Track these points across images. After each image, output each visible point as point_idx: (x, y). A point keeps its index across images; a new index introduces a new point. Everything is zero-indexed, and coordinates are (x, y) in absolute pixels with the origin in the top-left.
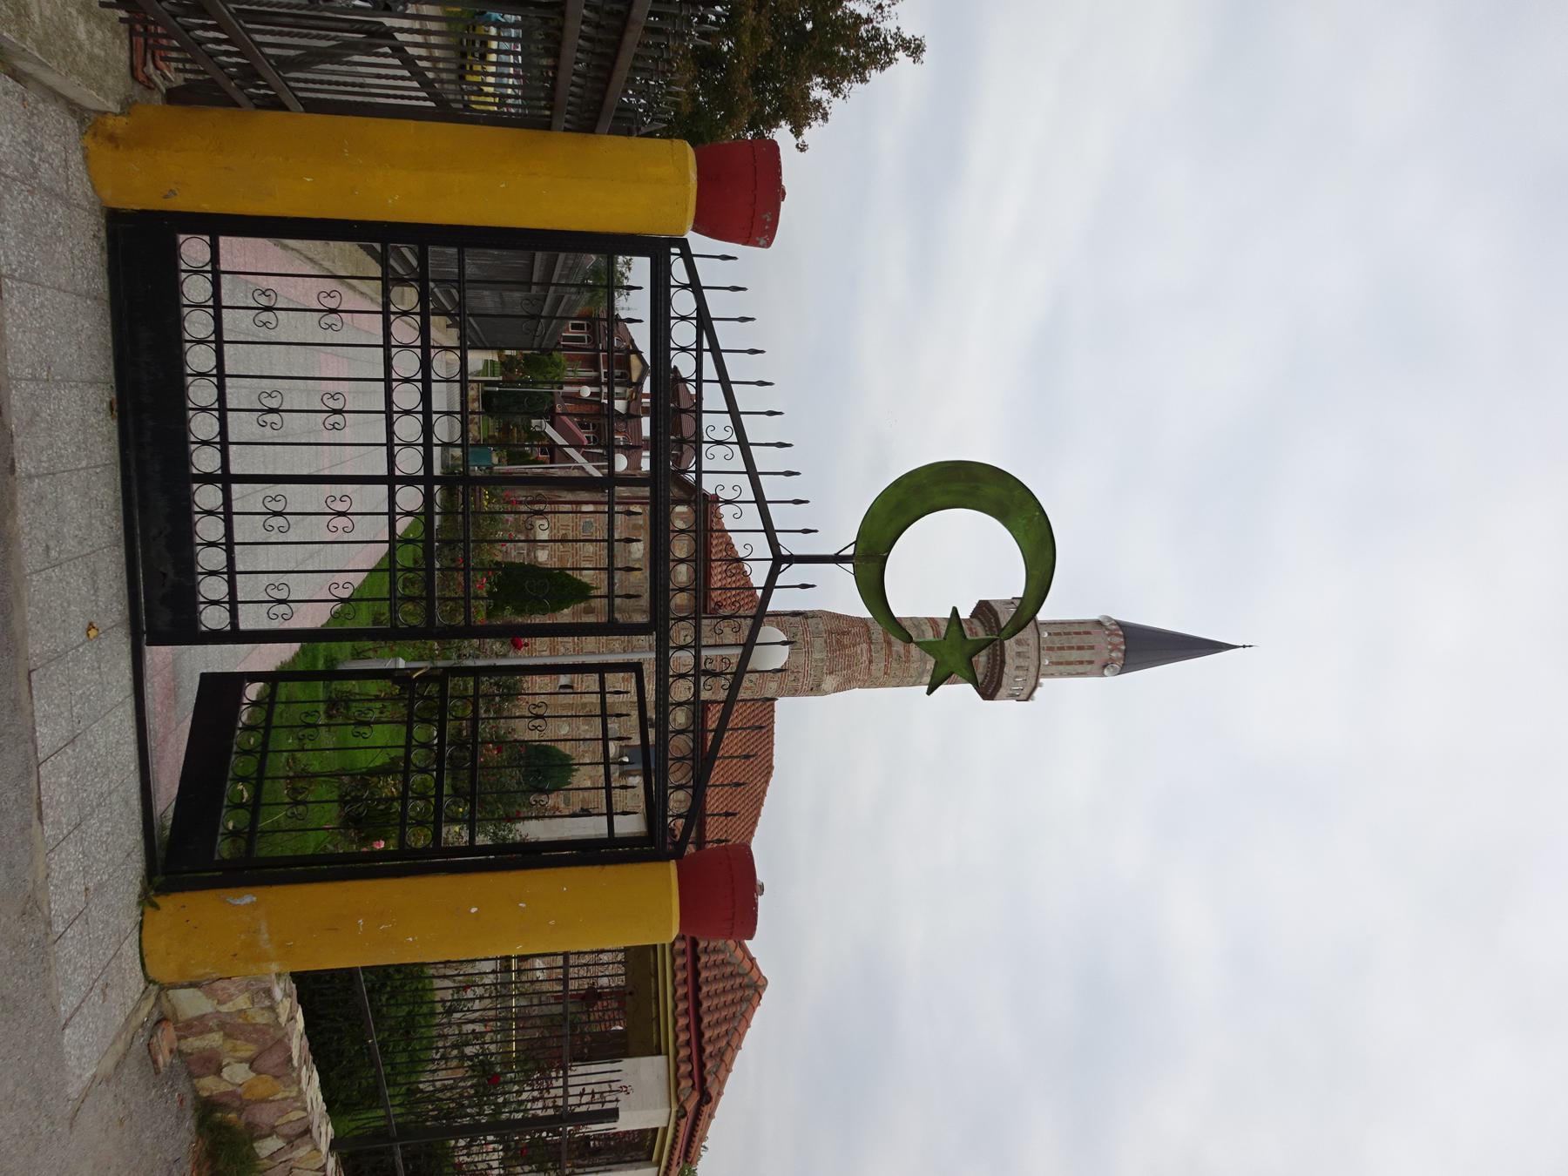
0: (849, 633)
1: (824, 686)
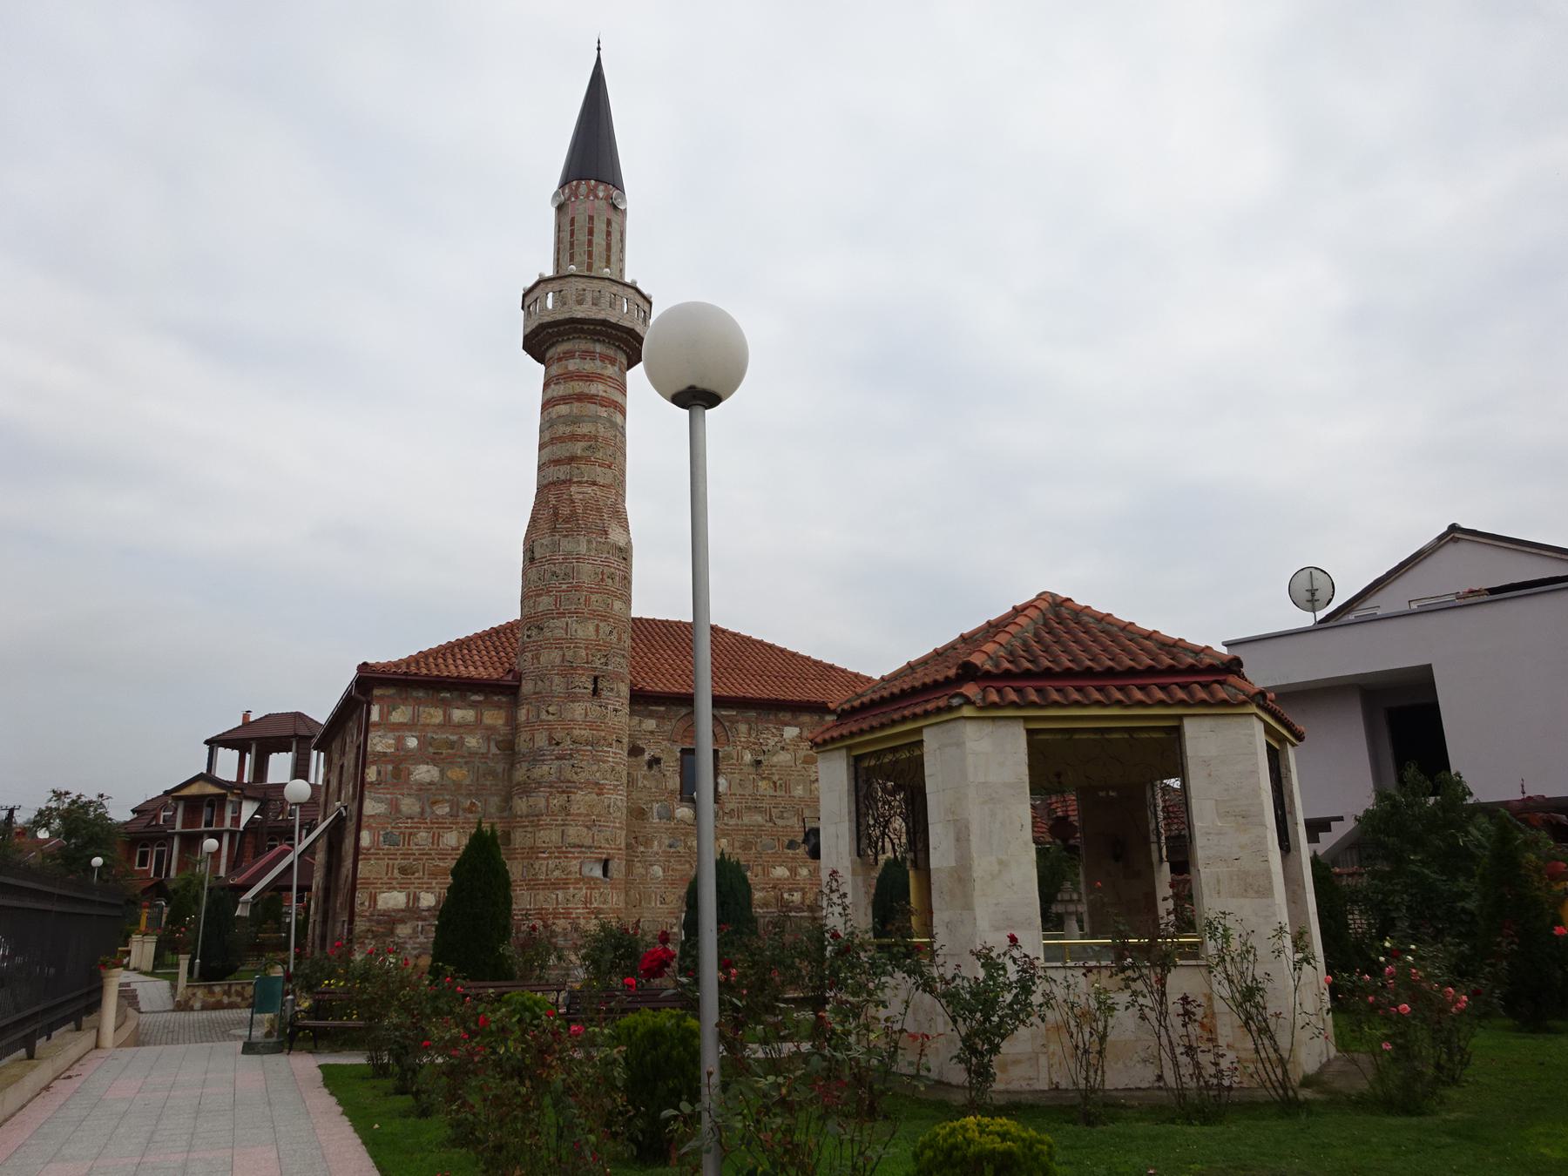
0: (555, 508)
1: (622, 544)
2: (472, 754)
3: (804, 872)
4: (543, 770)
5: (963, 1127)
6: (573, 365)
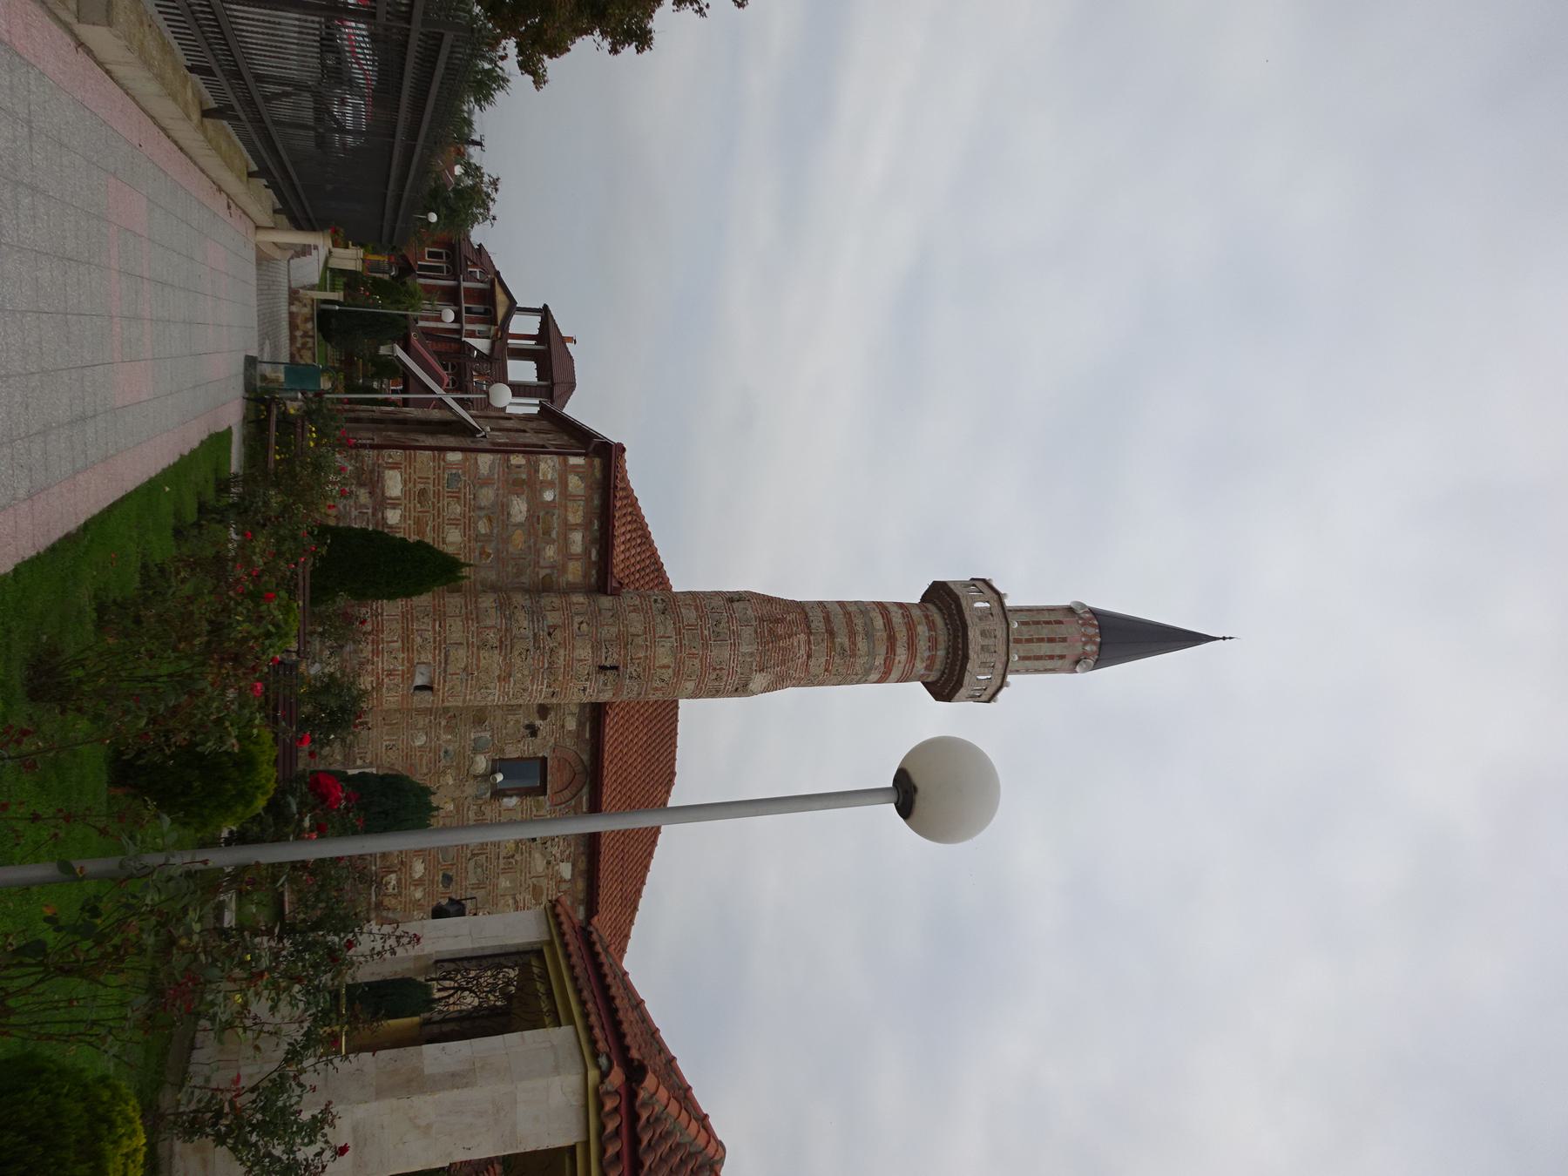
0: (783, 620)
1: (752, 686)
2: (538, 552)
3: (418, 894)
4: (523, 623)
5: (134, 1131)
6: (922, 630)
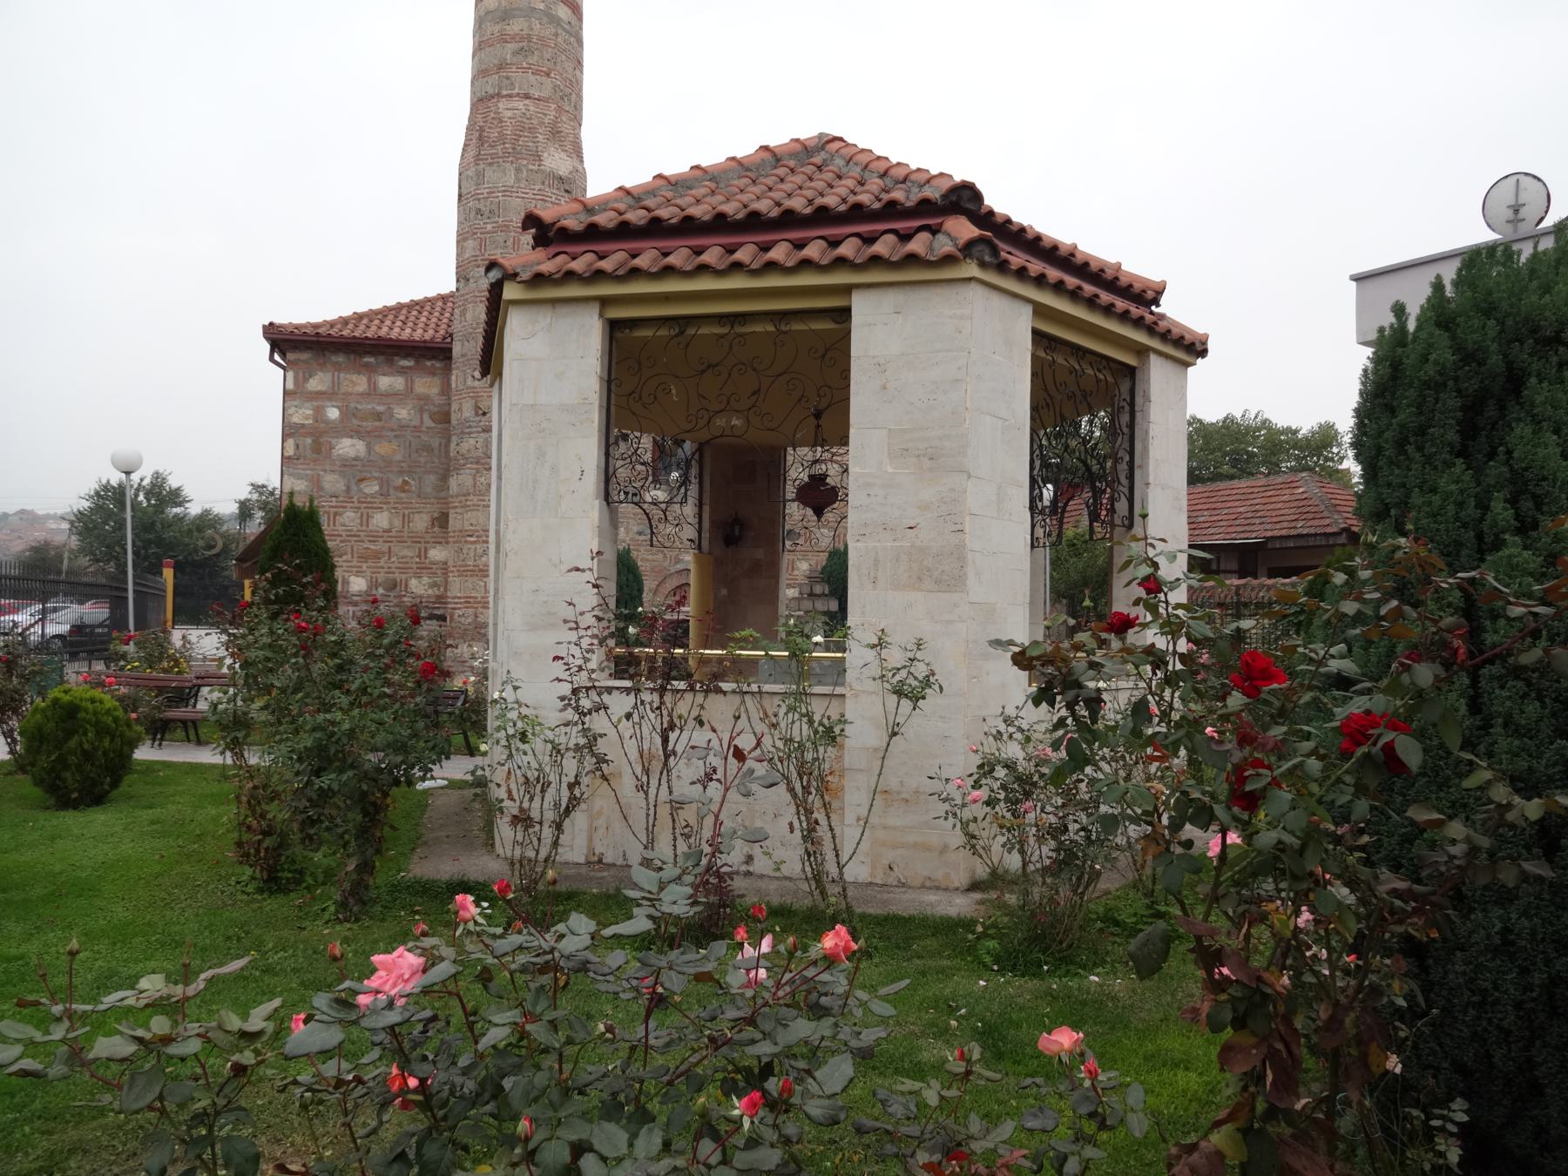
2: (402, 427)
